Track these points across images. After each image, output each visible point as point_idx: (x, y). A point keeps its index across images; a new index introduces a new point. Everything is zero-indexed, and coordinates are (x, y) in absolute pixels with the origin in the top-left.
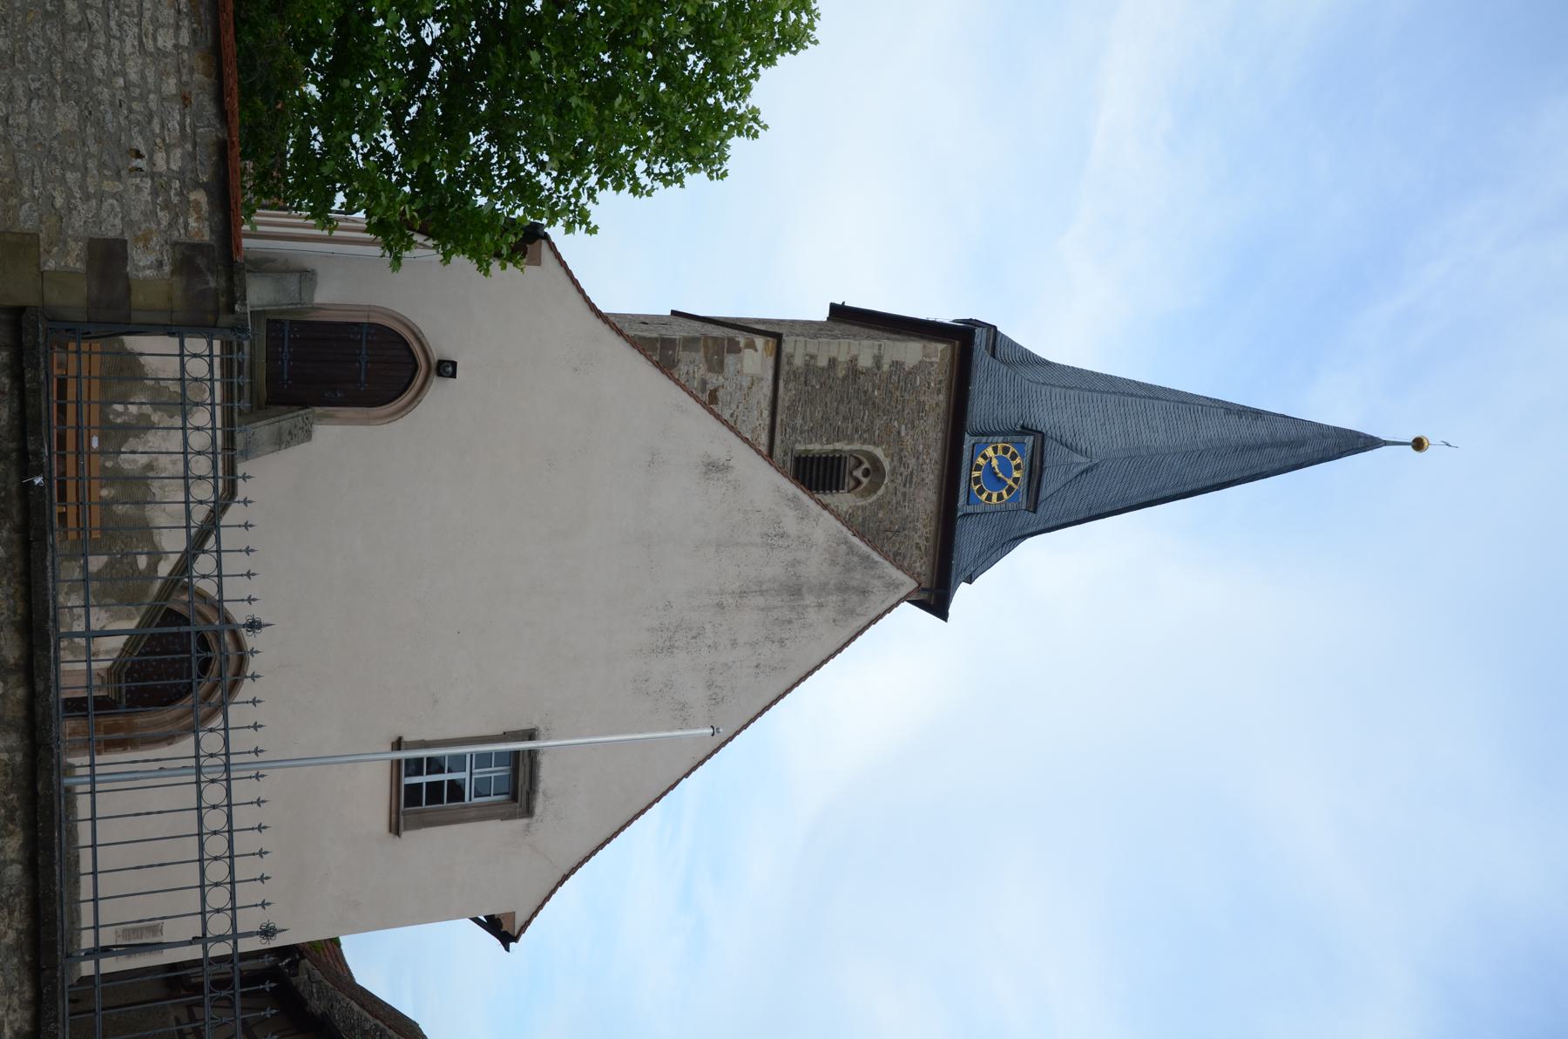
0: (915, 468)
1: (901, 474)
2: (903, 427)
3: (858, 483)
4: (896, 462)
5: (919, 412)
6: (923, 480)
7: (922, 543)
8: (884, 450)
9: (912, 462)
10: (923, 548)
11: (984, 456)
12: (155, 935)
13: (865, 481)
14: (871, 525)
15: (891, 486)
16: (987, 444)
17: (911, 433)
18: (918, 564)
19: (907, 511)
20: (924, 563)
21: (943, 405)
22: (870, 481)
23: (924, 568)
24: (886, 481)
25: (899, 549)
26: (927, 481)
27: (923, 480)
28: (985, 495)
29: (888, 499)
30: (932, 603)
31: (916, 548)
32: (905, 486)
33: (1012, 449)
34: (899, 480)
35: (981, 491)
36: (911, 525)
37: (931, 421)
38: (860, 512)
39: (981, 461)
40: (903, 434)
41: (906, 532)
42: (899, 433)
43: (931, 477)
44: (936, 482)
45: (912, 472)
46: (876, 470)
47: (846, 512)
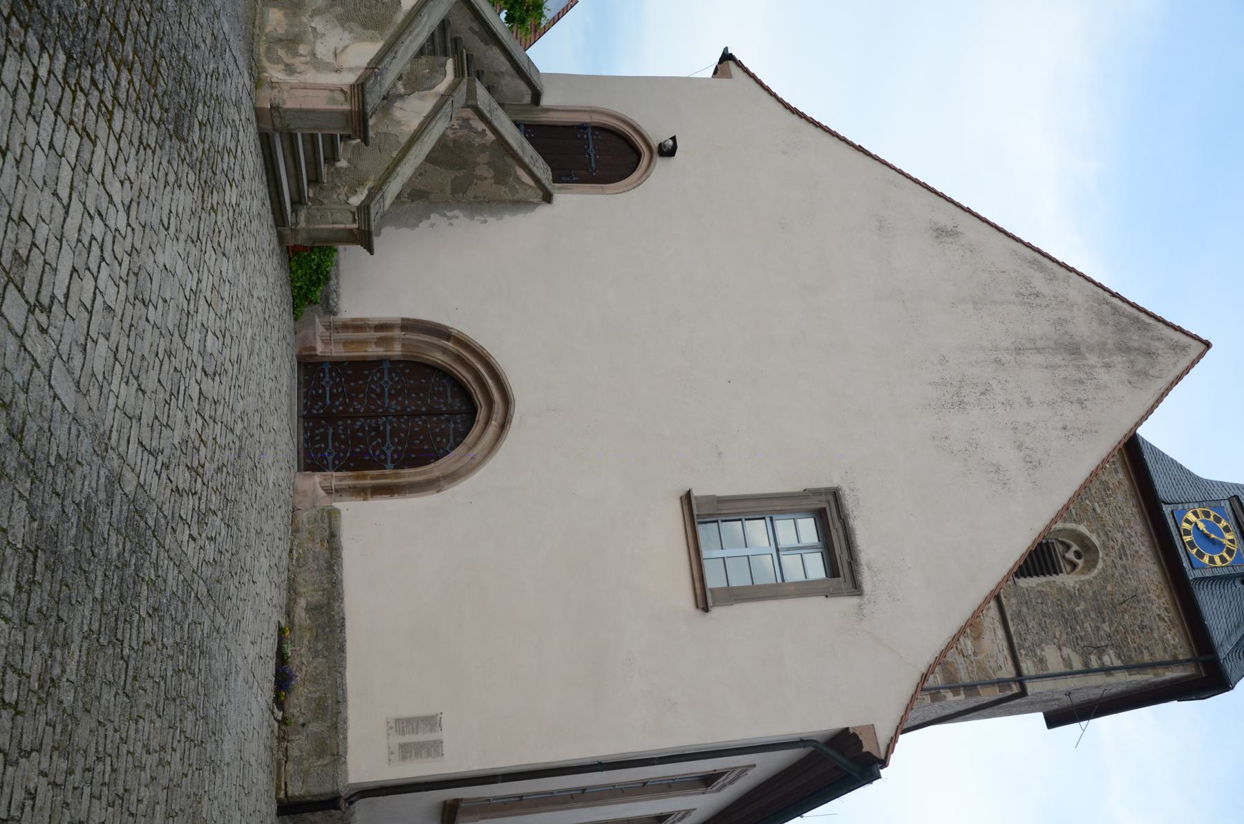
0: (1124, 541)
1: (1113, 548)
2: (1096, 505)
3: (1074, 566)
4: (1103, 537)
5: (1105, 490)
6: (1137, 552)
7: (1164, 614)
8: (1087, 526)
9: (1119, 536)
10: (1166, 619)
11: (1188, 521)
12: (432, 730)
13: (1080, 562)
14: (1104, 598)
15: (1108, 560)
16: (1185, 511)
17: (1106, 509)
18: (1169, 636)
19: (1135, 584)
20: (1175, 634)
21: (1126, 483)
22: (1086, 562)
23: (1177, 640)
24: (1101, 555)
25: (1142, 621)
26: (1141, 553)
27: (1137, 552)
28: (1206, 560)
29: (1109, 572)
30: (1204, 675)
31: (1160, 619)
32: (1121, 558)
33: (1212, 513)
34: (1113, 554)
35: (1201, 555)
36: (1144, 597)
37: (1120, 497)
38: (1087, 587)
39: (1186, 526)
40: (1099, 511)
41: (1142, 604)
42: (1094, 510)
43: (1143, 548)
44: (1150, 553)
45: (1122, 545)
46: (1087, 549)
47: (1074, 588)
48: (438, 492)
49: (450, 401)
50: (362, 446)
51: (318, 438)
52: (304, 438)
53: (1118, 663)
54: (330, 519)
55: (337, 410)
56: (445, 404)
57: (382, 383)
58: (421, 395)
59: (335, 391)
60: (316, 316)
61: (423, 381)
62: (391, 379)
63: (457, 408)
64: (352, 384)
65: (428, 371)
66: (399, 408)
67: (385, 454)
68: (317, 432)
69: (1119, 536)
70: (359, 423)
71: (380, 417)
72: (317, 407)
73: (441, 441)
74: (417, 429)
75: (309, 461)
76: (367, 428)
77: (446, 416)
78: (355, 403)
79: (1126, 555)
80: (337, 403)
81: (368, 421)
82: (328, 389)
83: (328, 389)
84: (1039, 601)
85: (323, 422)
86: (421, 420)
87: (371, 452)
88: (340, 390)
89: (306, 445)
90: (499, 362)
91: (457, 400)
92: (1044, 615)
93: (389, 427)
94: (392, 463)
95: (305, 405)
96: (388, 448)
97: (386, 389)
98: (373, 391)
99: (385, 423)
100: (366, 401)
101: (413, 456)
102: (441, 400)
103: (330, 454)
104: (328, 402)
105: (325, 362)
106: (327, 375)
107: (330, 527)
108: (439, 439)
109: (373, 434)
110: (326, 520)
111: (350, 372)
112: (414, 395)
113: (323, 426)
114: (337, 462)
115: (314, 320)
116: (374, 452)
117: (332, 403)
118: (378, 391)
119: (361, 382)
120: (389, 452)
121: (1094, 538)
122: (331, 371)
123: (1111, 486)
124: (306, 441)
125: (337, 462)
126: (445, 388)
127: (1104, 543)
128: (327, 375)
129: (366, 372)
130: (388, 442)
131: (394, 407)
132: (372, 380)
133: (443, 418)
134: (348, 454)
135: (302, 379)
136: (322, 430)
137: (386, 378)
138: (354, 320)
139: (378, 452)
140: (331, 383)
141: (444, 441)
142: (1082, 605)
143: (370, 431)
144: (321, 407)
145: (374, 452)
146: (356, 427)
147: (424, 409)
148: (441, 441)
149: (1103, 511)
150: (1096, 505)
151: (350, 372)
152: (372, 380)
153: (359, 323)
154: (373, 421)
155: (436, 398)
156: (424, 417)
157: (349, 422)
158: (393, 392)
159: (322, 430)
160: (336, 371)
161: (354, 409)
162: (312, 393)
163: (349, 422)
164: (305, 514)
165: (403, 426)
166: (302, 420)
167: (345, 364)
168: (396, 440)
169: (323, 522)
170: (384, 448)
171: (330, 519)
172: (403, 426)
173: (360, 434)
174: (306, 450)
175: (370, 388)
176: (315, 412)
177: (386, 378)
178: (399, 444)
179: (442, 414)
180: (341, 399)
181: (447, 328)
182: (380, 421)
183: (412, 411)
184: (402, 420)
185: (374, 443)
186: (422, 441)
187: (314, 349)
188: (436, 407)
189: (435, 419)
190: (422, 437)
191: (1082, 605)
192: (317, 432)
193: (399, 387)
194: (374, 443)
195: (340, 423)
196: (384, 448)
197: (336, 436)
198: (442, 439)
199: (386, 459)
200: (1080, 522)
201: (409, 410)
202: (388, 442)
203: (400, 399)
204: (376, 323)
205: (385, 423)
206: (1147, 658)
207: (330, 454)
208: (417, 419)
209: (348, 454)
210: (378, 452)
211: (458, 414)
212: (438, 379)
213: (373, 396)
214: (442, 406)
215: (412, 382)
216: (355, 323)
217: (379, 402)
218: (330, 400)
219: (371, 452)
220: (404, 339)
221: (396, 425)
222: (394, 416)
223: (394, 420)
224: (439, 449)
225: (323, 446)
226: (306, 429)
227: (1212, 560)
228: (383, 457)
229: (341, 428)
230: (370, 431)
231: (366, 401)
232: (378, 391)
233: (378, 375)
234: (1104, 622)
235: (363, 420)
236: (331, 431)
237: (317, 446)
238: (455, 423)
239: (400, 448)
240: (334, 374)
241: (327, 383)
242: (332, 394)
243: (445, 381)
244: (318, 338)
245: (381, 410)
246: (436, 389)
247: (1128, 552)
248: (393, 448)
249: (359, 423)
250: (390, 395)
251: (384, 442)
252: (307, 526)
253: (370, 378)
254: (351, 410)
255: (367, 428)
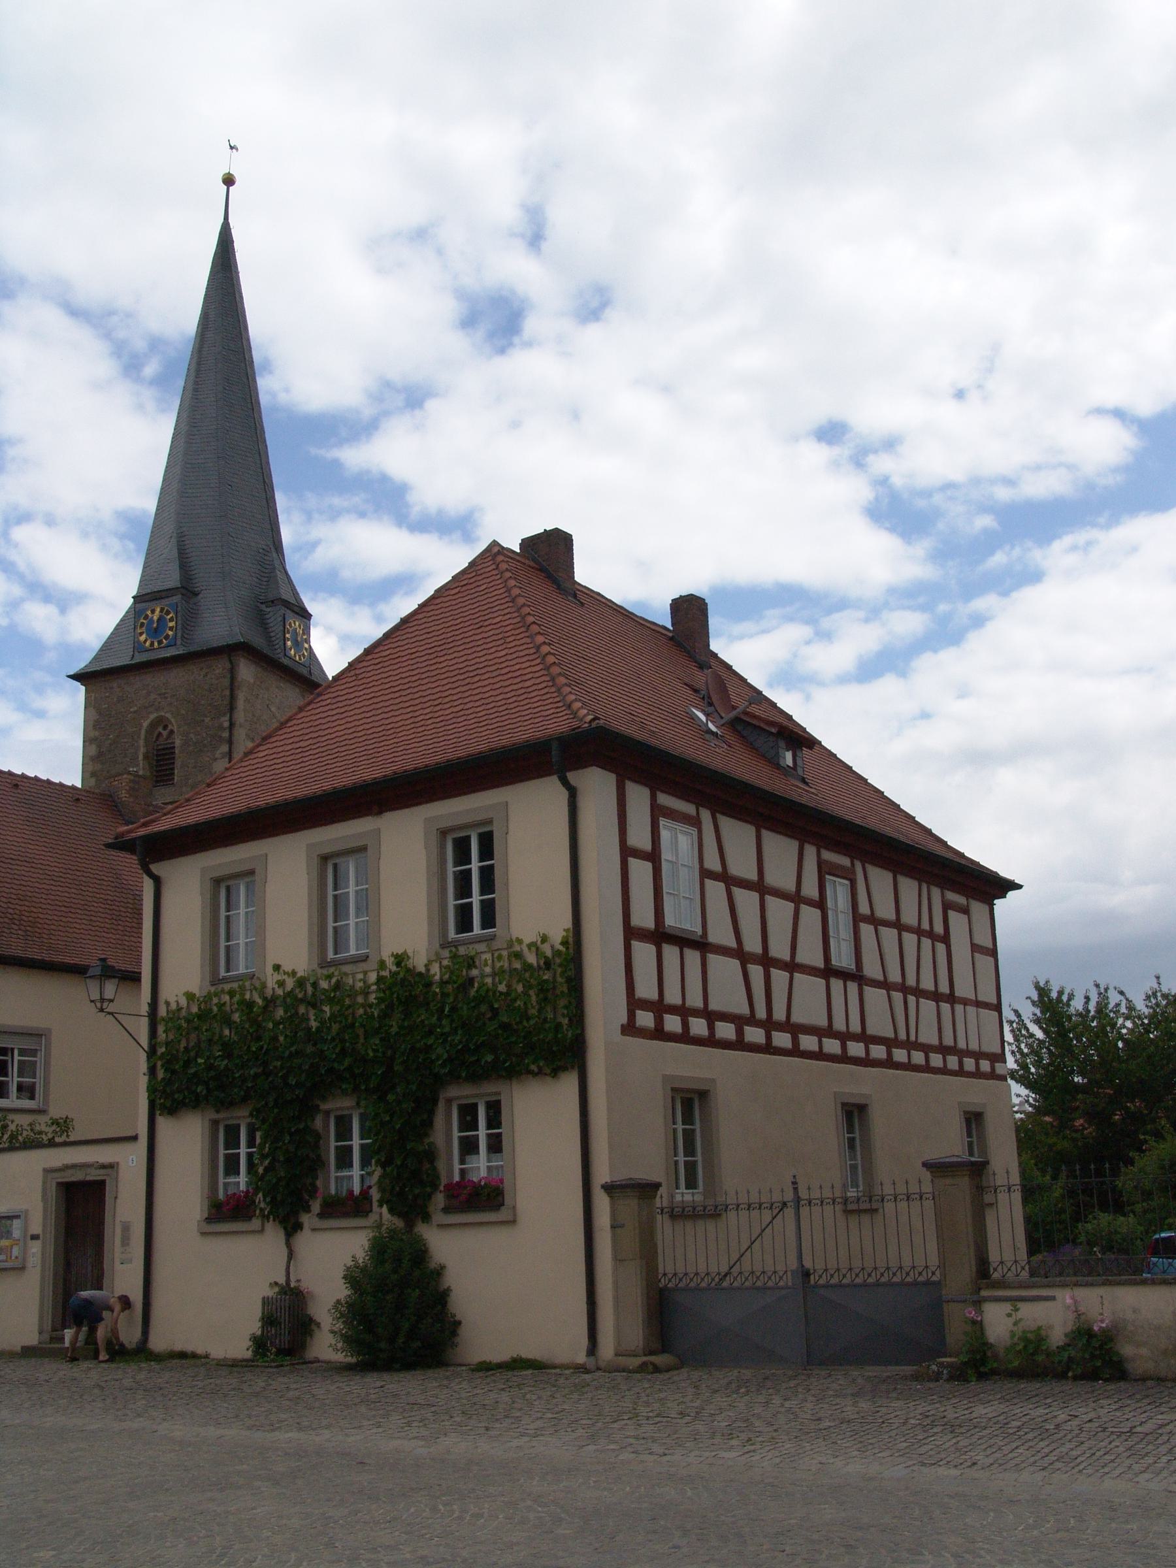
1: (159, 703)
2: (131, 710)
9: (153, 696)
24: (163, 714)
26: (165, 681)
28: (170, 633)
35: (167, 637)
39: (148, 644)
40: (136, 708)
42: (135, 712)
46: (161, 722)
53: (227, 718)
69: (153, 696)
79: (165, 693)
84: (186, 769)
92: (195, 767)
121: (153, 716)
123: (121, 695)
127: (157, 710)
142: (192, 735)
149: (136, 705)
150: (131, 710)
191: (192, 735)
200: (141, 725)
206: (227, 693)
227: (171, 629)
234: (203, 721)
247: (164, 691)
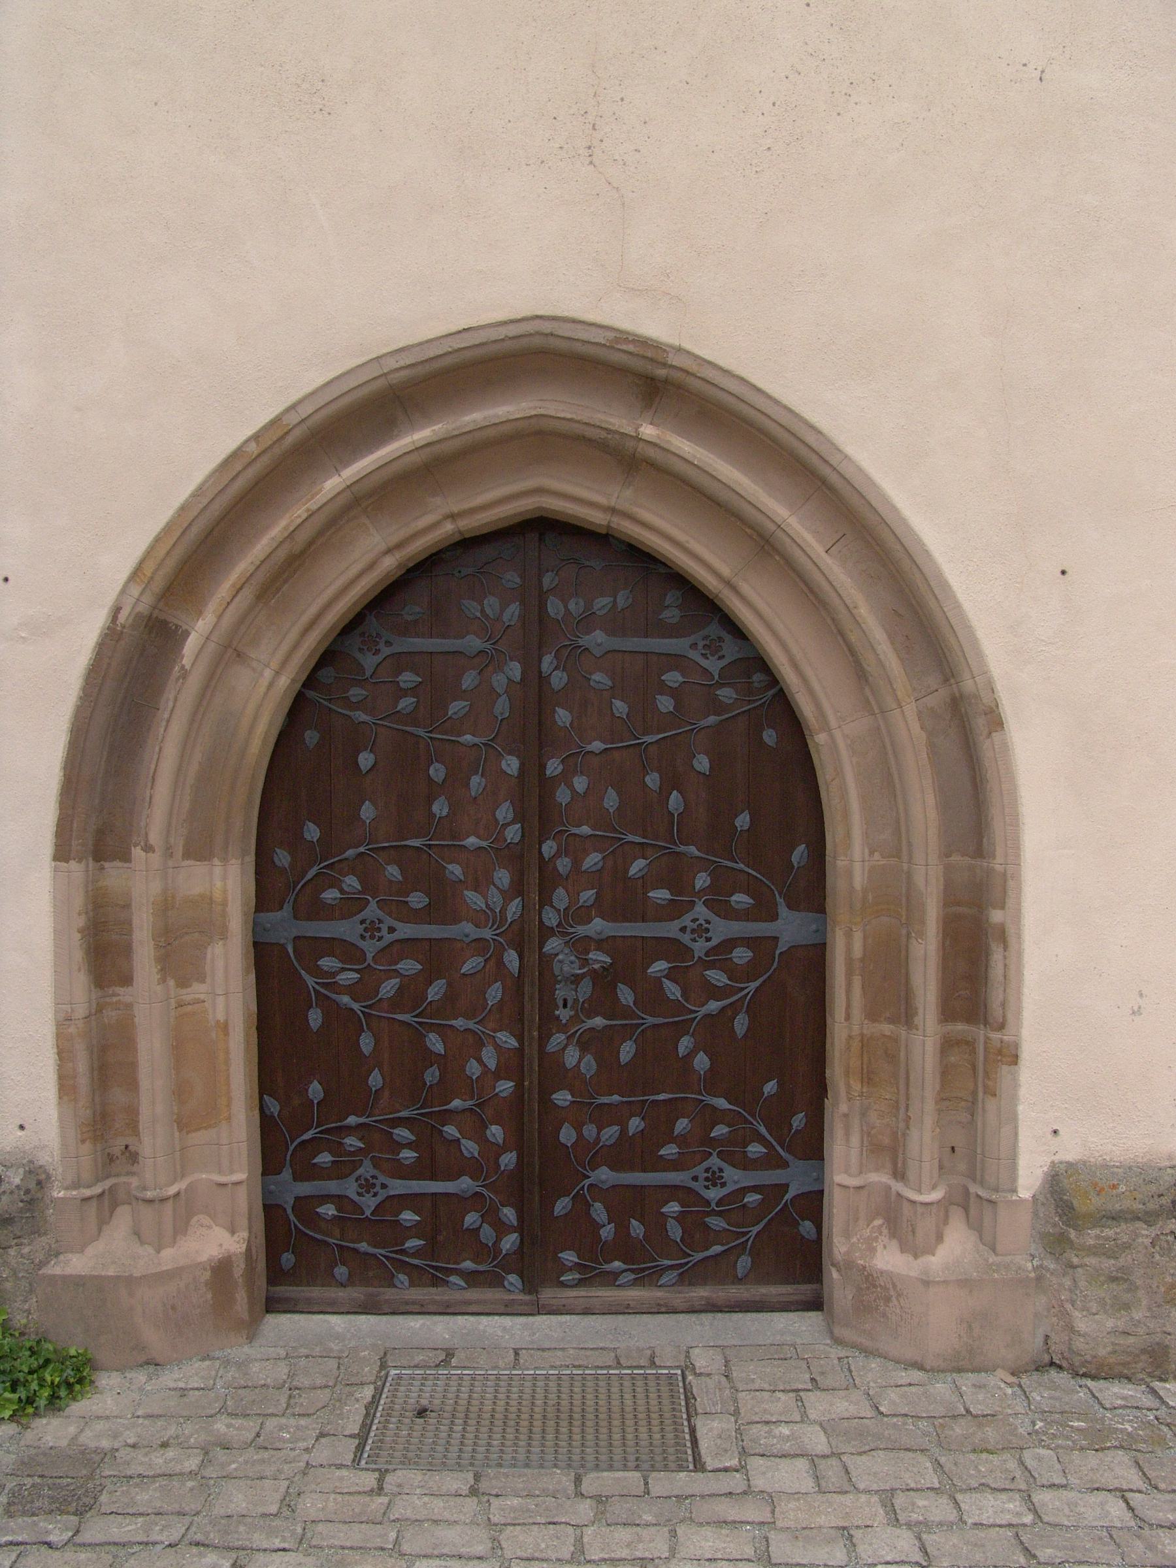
48: (996, 722)
49: (473, 643)
50: (685, 1044)
51: (637, 1229)
52: (635, 1283)
54: (1115, 1218)
55: (504, 1149)
56: (489, 660)
57: (370, 948)
58: (437, 772)
59: (408, 1155)
60: (55, 1269)
61: (365, 760)
62: (351, 906)
63: (513, 612)
64: (375, 1080)
65: (311, 737)
66: (503, 877)
67: (730, 944)
68: (608, 1232)
70: (572, 1057)
71: (546, 961)
72: (487, 1233)
73: (674, 693)
74: (611, 800)
75: (744, 1263)
76: (599, 1021)
77: (547, 662)
78: (473, 1069)
80: (470, 1147)
81: (564, 1014)
82: (399, 1187)
83: (399, 1187)
85: (562, 1206)
86: (565, 777)
87: (713, 1006)
88: (403, 1134)
89: (669, 1277)
90: (315, 378)
91: (472, 607)
93: (598, 926)
94: (774, 917)
95: (472, 1279)
96: (701, 931)
97: (406, 930)
98: (409, 997)
99: (581, 946)
100: (459, 1023)
101: (743, 821)
102: (469, 680)
103: (714, 1179)
104: (465, 1184)
105: (266, 1193)
106: (332, 1187)
107: (1148, 1218)
108: (665, 704)
109: (626, 995)
110: (1121, 1232)
111: (316, 1090)
112: (440, 808)
113: (582, 1204)
114: (755, 1149)
115: (79, 1282)
116: (715, 992)
117: (473, 1168)
118: (409, 966)
119: (366, 1043)
120: (722, 929)
122: (306, 1172)
124: (647, 1277)
125: (755, 1149)
126: (401, 661)
128: (332, 1187)
129: (315, 1018)
130: (669, 929)
131: (495, 898)
132: (352, 990)
133: (558, 679)
134: (722, 1103)
135: (341, 1294)
136: (599, 1211)
137: (346, 929)
138: (66, 1086)
139: (718, 977)
140: (366, 1169)
141: (673, 678)
143: (613, 1009)
144: (491, 1216)
145: (715, 992)
146: (589, 1066)
147: (511, 765)
148: (674, 693)
151: (316, 1090)
152: (352, 990)
153: (82, 1066)
154: (561, 992)
155: (456, 707)
156: (553, 767)
157: (562, 1098)
158: (417, 900)
159: (599, 1211)
160: (314, 1146)
161: (498, 1075)
162: (418, 1253)
163: (562, 1098)
164: (1082, 1325)
165: (592, 860)
166: (548, 1295)
167: (274, 1107)
168: (661, 895)
169: (1127, 1247)
170: (700, 947)
171: (1115, 1218)
172: (592, 860)
173: (627, 1051)
174: (689, 1276)
175: (396, 1003)
176: (509, 1242)
177: (346, 929)
178: (676, 879)
179: (543, 680)
180: (451, 1130)
181: (111, 635)
182: (566, 963)
183: (520, 816)
184: (563, 865)
185: (673, 990)
186: (672, 782)
187: (221, 1269)
188: (502, 707)
189: (563, 716)
190: (652, 780)
192: (608, 1232)
193: (393, 871)
194: (673, 990)
195: (567, 1135)
196: (700, 947)
197: (621, 1154)
198: (663, 688)
199: (750, 942)
201: (513, 833)
202: (669, 929)
203: (455, 870)
204: (81, 981)
205: (581, 946)
207: (714, 1179)
208: (563, 796)
209: (722, 1103)
210: (718, 977)
211: (542, 606)
212: (356, 693)
213: (436, 991)
214: (499, 681)
215: (367, 811)
216: (83, 1082)
217: (471, 965)
218: (452, 1176)
219: (713, 1006)
220: (169, 852)
221: (587, 896)
222: (545, 899)
223: (561, 897)
224: (717, 707)
225: (674, 1208)
226: (591, 1276)
228: (741, 955)
229: (590, 1131)
230: (613, 1009)
231: (459, 1023)
232: (409, 966)
233: (327, 963)
235: (558, 1039)
236: (604, 1175)
237: (675, 1231)
238: (587, 621)
239: (702, 880)
240: (324, 1158)
241: (367, 1186)
242: (427, 1169)
243: (369, 662)
244: (170, 1257)
245: (512, 959)
246: (406, 703)
248: (701, 910)
249: (572, 1057)
250: (433, 913)
251: (672, 949)
252: (1137, 1315)
253: (345, 999)
254: (505, 1087)
255: (599, 1021)
